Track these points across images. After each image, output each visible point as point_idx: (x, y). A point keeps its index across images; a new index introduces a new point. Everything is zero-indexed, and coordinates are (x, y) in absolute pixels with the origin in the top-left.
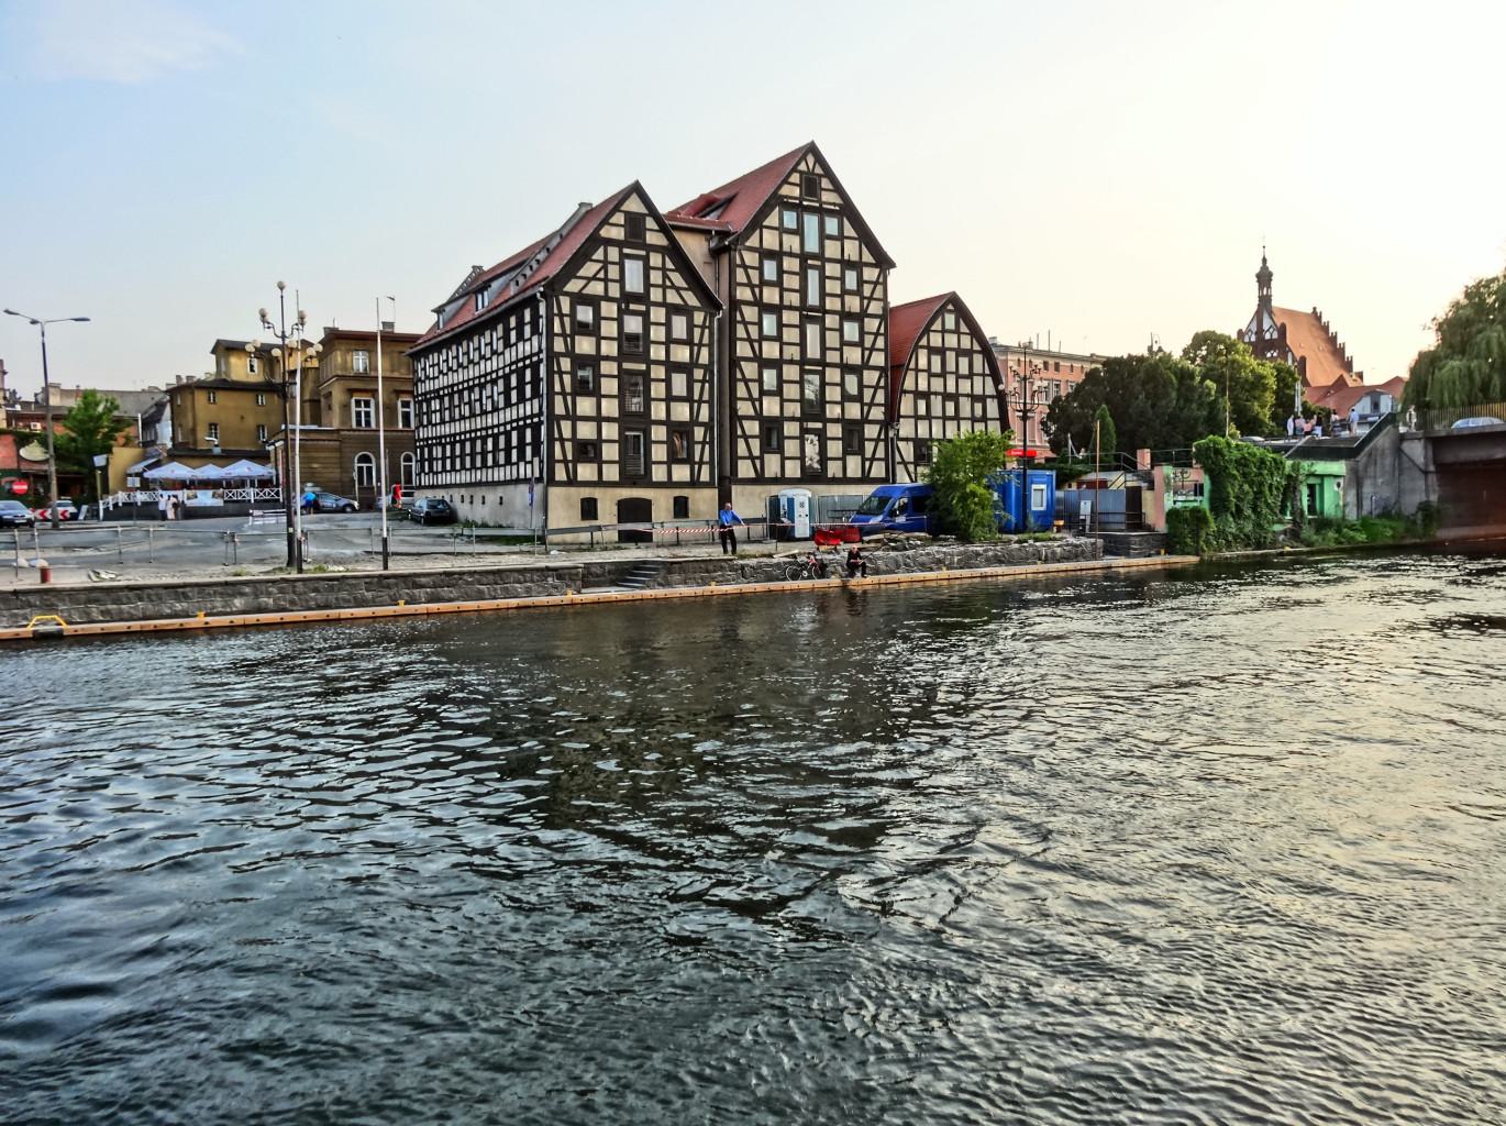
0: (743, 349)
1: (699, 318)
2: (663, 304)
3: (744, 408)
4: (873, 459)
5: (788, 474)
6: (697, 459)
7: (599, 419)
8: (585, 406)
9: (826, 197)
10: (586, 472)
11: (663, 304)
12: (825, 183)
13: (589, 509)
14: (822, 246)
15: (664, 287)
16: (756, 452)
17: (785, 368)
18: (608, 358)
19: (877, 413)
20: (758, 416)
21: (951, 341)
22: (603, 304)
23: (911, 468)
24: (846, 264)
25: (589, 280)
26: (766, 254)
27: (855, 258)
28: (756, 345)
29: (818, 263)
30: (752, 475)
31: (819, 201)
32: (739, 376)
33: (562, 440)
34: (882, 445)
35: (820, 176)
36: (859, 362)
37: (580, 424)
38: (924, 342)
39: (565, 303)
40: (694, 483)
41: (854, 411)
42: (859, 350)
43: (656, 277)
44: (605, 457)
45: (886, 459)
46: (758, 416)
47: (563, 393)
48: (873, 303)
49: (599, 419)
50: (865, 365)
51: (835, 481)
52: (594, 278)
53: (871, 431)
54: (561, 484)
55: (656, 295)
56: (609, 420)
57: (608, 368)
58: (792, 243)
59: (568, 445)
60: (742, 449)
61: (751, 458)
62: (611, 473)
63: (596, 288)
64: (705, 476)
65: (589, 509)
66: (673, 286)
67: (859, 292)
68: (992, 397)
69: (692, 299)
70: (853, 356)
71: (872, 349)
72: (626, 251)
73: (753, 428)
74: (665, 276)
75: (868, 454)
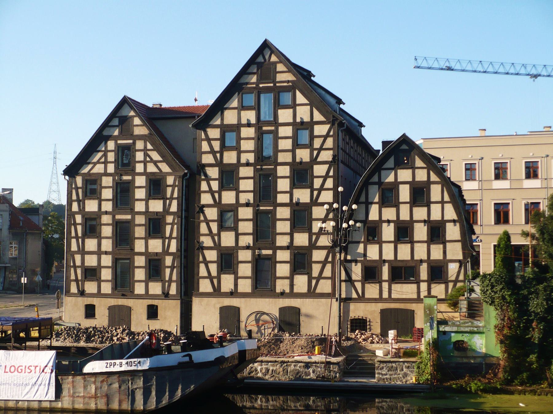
0: (206, 199)
1: (170, 180)
2: (145, 173)
3: (207, 241)
4: (320, 277)
5: (240, 289)
6: (167, 279)
7: (99, 253)
8: (91, 244)
9: (280, 77)
10: (90, 287)
11: (145, 173)
12: (280, 67)
13: (90, 311)
14: (276, 116)
15: (145, 163)
16: (214, 273)
17: (241, 210)
18: (106, 213)
19: (325, 241)
20: (217, 246)
21: (405, 175)
22: (104, 179)
23: (358, 285)
24: (299, 126)
25: (95, 164)
26: (225, 129)
27: (307, 119)
28: (217, 195)
29: (273, 128)
30: (210, 289)
31: (275, 82)
32: (202, 218)
33: (75, 267)
34: (329, 267)
35: (275, 63)
36: (308, 200)
37: (87, 257)
38: (375, 179)
39: (79, 180)
40: (166, 295)
41: (301, 239)
42: (308, 191)
43: (140, 156)
44: (103, 278)
45: (333, 278)
46: (217, 246)
47: (77, 237)
48: (323, 153)
49: (99, 253)
50: (314, 202)
51: (283, 294)
52: (98, 162)
53: (318, 255)
54: (74, 295)
55: (139, 168)
56: (106, 253)
57: (106, 219)
58: (250, 116)
59: (79, 271)
60: (203, 271)
61: (210, 277)
62: (107, 288)
63: (99, 169)
64: (173, 290)
65: (90, 311)
66: (152, 161)
67: (310, 146)
68: (454, 221)
69: (165, 168)
70: (303, 195)
71: (322, 189)
72: (119, 142)
73: (212, 255)
74: (146, 155)
75: (315, 273)
